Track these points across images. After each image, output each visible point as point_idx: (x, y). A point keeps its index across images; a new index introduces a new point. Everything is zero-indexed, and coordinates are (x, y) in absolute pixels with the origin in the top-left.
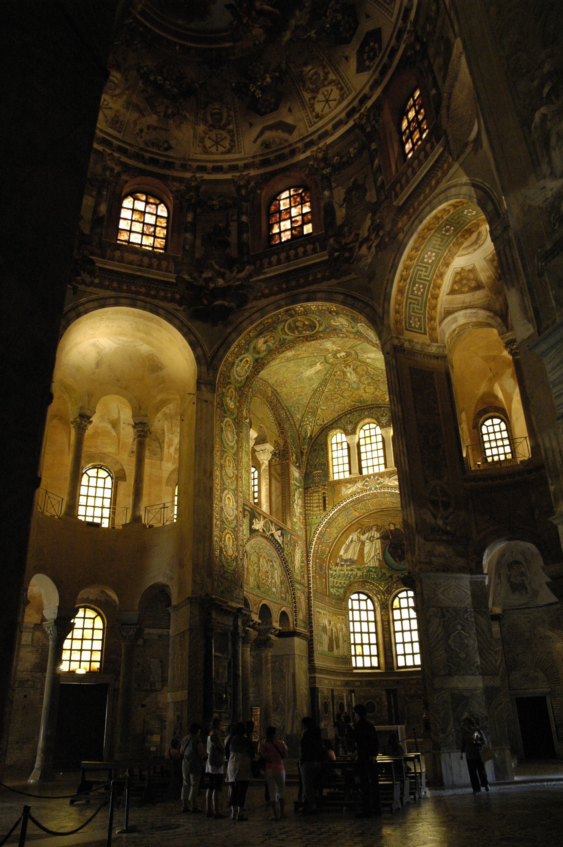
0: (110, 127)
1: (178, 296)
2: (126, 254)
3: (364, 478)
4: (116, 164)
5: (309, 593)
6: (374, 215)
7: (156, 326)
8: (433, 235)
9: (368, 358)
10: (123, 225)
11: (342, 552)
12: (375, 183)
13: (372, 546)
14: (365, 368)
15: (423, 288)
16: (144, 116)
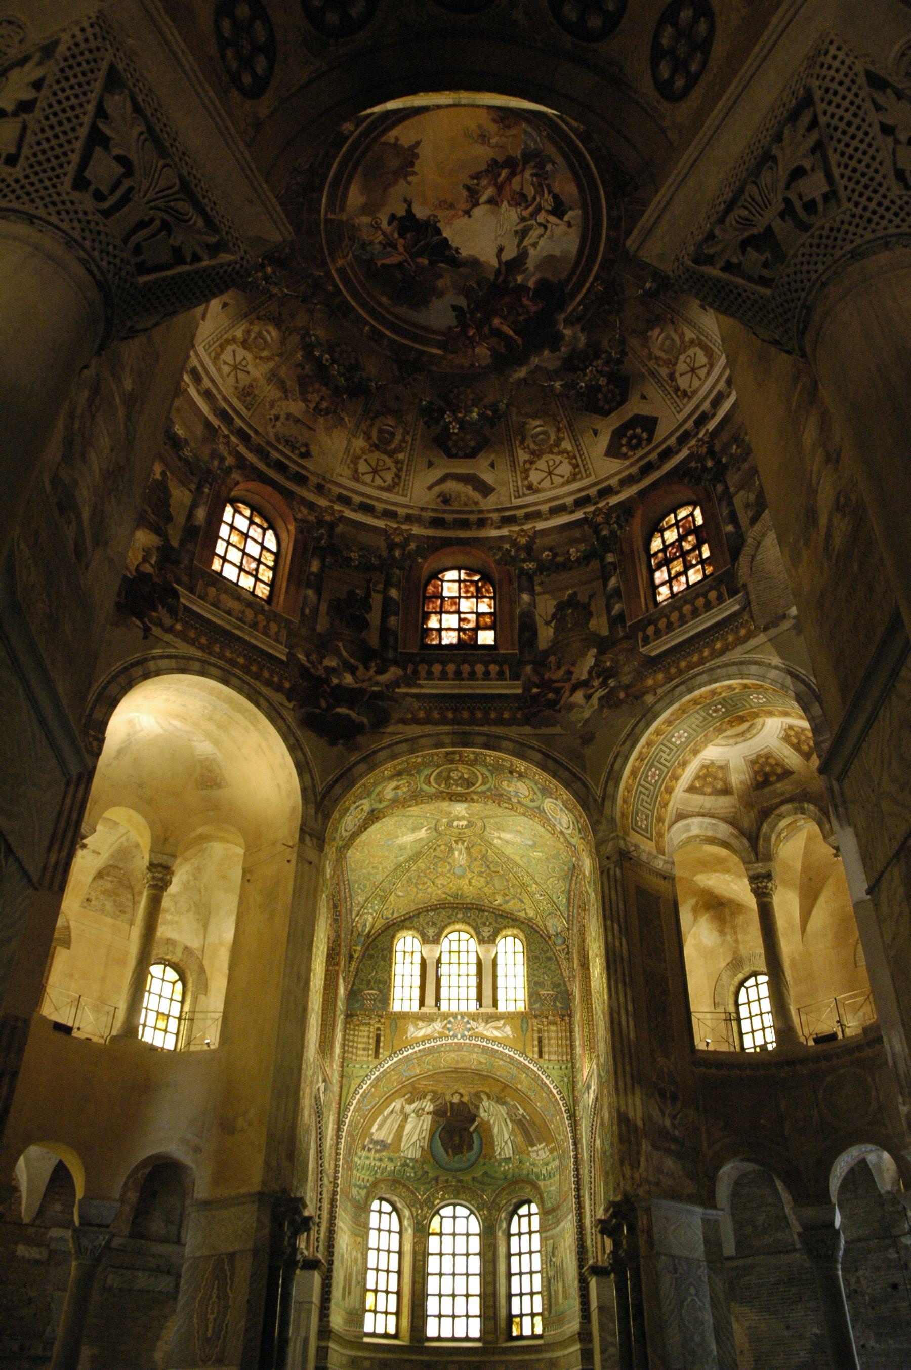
0: (238, 398)
1: (287, 685)
2: (224, 597)
3: (445, 1016)
4: (230, 453)
5: (334, 1193)
6: (601, 652)
7: (245, 722)
8: (697, 712)
9: (499, 838)
10: (220, 548)
11: (373, 1130)
12: (609, 611)
13: (417, 1124)
14: (484, 849)
15: (660, 776)
16: (287, 398)
